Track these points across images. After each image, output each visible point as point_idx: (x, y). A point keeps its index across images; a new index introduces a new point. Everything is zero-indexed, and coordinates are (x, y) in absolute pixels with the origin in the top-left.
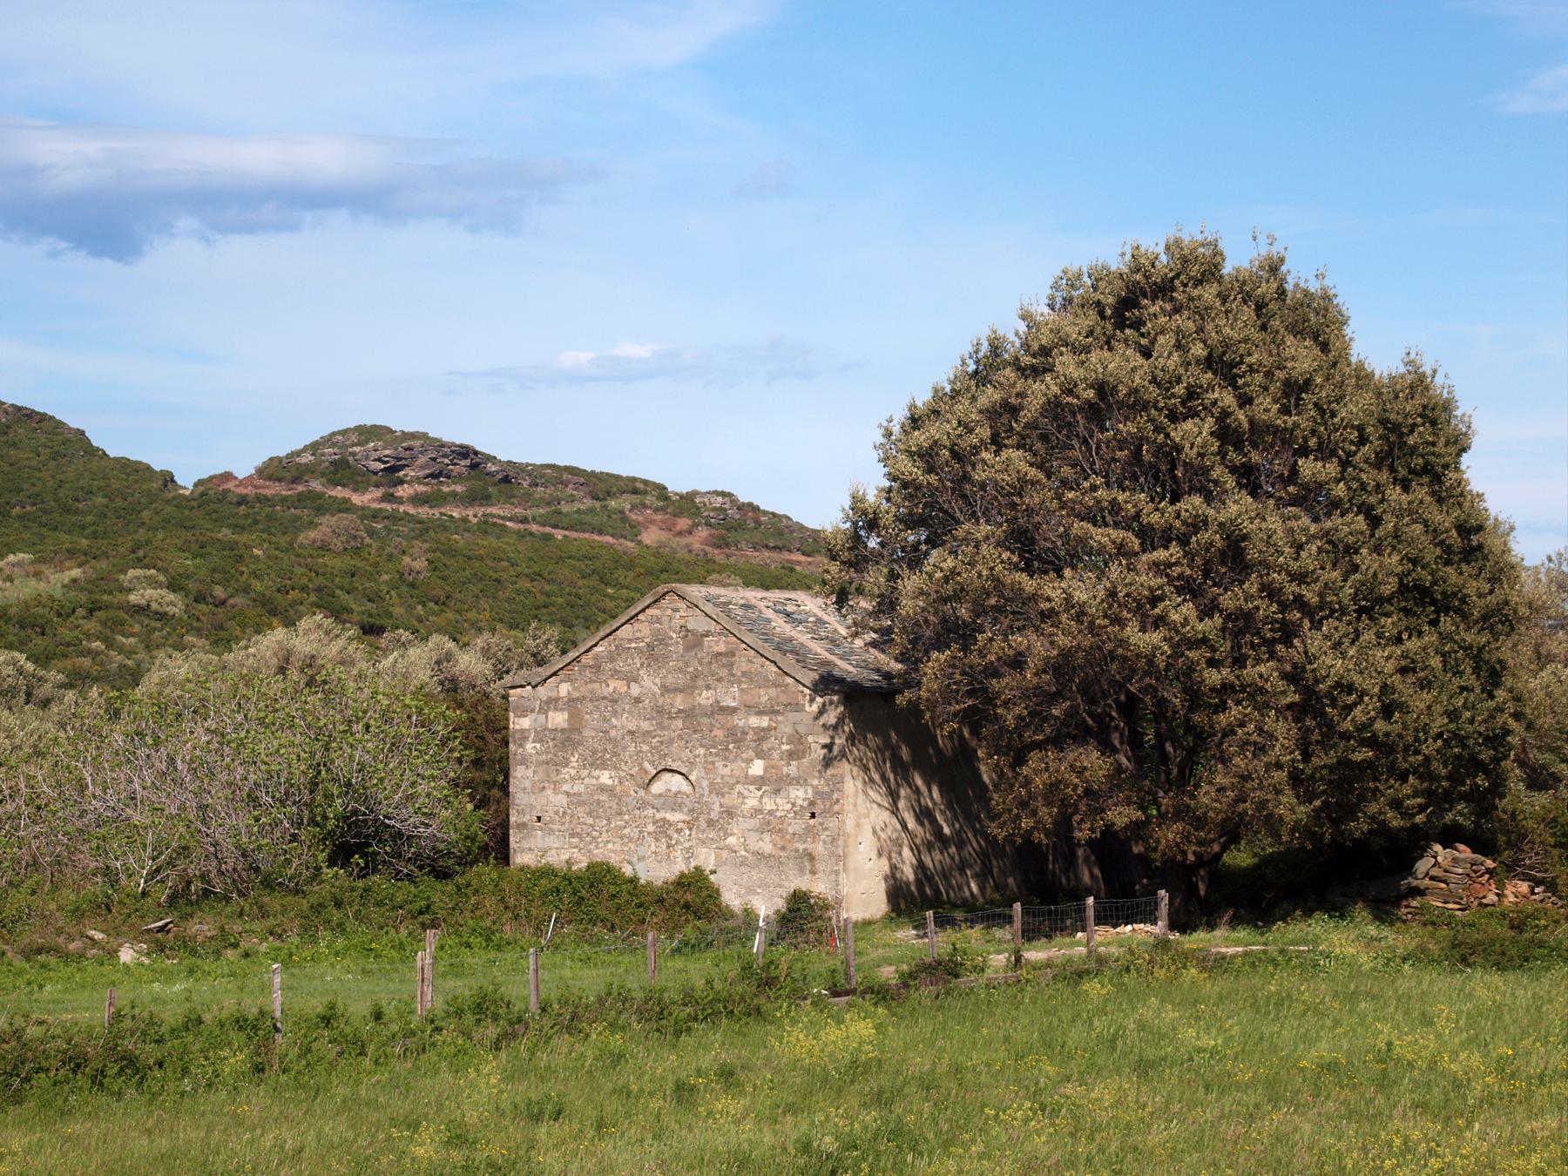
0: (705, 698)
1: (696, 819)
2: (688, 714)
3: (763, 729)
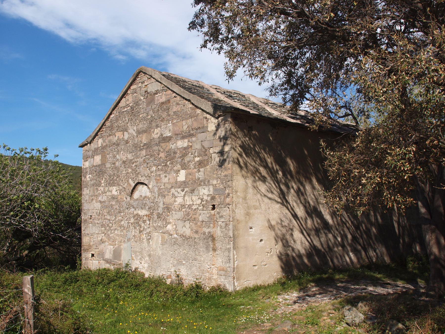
0: (156, 133)
1: (152, 214)
2: (148, 146)
3: (185, 149)
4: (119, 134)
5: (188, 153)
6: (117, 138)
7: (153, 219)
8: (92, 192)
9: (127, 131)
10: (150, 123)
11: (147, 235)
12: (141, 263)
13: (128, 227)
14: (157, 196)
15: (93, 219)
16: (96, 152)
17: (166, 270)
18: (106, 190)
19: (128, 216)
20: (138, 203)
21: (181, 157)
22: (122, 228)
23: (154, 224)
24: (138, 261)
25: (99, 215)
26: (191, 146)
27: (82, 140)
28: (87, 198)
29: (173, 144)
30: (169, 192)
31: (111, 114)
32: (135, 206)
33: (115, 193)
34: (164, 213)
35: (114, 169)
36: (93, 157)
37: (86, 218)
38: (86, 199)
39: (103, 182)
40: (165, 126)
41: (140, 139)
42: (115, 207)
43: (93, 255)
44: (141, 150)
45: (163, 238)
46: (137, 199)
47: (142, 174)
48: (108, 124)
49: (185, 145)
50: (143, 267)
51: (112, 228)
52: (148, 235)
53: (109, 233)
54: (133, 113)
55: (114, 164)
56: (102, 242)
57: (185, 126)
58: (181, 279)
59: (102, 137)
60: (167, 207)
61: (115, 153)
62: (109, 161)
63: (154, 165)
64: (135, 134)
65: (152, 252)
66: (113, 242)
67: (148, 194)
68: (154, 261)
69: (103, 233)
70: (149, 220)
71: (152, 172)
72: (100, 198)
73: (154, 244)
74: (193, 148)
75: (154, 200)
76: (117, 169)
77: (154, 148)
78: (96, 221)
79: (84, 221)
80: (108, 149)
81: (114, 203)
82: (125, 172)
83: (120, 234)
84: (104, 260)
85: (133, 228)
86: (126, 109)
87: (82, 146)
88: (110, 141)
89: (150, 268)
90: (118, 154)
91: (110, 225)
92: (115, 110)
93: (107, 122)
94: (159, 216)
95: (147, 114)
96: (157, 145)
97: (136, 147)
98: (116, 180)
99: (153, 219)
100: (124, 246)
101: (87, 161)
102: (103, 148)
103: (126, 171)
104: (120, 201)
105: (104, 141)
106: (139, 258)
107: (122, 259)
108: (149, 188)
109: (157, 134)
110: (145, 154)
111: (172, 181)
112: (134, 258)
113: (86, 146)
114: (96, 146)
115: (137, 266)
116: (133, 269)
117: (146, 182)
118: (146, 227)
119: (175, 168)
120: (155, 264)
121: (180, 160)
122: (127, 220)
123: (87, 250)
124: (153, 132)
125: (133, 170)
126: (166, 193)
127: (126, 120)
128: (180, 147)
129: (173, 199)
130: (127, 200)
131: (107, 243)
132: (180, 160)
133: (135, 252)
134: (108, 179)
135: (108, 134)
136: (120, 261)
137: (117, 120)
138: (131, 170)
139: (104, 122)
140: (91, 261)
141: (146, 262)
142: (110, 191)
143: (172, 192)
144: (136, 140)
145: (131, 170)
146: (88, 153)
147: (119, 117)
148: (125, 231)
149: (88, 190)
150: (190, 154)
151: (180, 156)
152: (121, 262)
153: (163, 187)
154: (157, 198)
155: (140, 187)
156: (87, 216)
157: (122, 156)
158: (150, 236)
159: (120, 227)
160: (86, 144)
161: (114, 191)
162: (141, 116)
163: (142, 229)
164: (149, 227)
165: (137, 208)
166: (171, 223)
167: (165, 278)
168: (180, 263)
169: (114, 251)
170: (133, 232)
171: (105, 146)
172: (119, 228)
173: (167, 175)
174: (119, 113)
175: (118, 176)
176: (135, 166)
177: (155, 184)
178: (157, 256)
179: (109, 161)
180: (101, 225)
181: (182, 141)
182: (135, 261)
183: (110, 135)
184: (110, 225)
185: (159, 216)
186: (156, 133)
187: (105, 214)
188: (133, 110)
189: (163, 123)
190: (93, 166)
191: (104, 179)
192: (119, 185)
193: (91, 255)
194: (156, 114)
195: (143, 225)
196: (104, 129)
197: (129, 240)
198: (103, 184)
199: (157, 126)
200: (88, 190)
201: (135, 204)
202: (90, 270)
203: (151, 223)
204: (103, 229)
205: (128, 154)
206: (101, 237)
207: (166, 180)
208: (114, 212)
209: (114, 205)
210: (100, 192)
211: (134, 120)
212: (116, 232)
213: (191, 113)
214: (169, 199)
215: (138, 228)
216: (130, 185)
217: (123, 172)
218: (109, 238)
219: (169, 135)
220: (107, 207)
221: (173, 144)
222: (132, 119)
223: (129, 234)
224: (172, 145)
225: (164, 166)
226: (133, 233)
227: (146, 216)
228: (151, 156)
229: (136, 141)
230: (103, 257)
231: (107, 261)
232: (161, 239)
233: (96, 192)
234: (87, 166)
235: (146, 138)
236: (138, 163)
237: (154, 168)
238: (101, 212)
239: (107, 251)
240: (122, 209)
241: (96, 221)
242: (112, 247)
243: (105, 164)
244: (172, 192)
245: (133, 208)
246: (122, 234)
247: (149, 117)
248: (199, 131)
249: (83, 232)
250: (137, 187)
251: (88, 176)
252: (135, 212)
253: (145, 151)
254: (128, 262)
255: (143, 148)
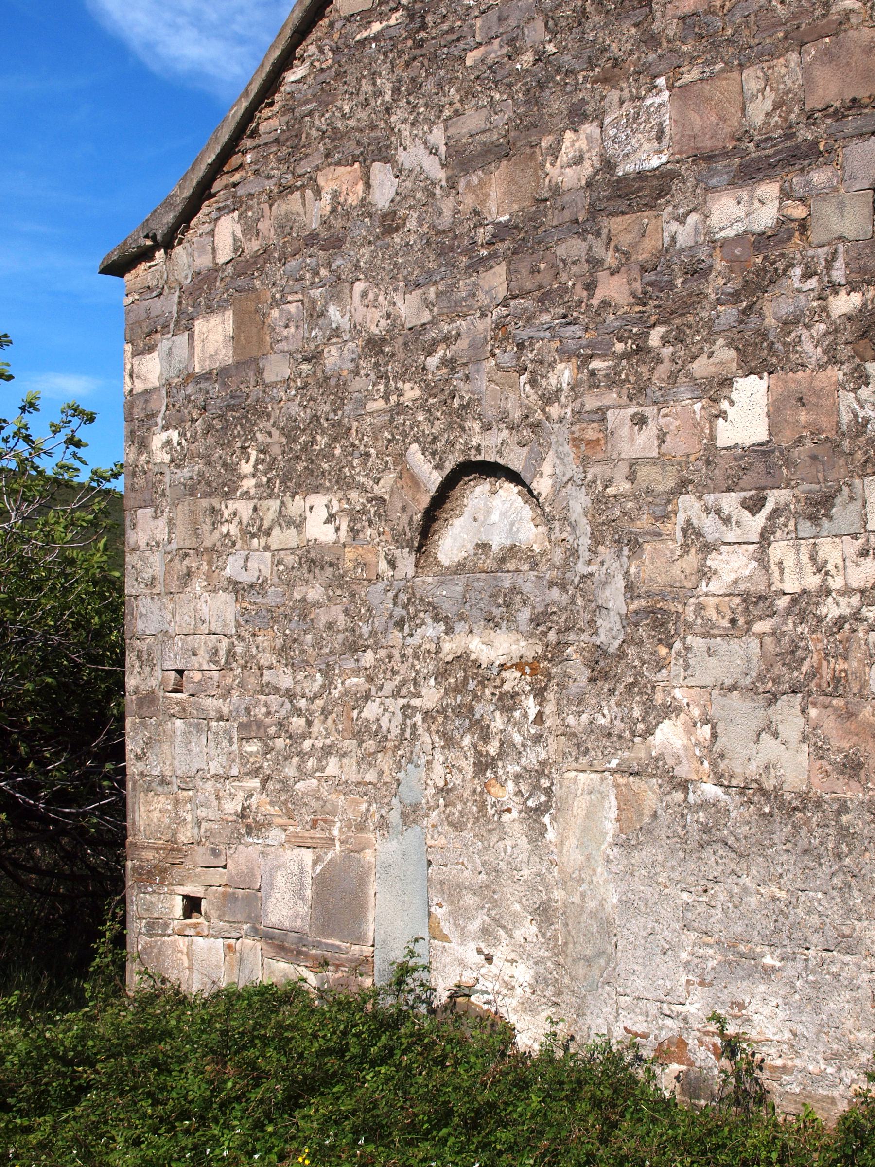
0: (571, 159)
1: (555, 653)
2: (521, 238)
3: (762, 241)
4: (339, 181)
5: (780, 265)
6: (325, 204)
7: (562, 686)
8: (181, 530)
9: (386, 160)
10: (533, 99)
11: (524, 788)
12: (489, 959)
13: (408, 736)
14: (585, 542)
15: (188, 687)
16: (202, 294)
17: (653, 1008)
18: (269, 517)
19: (403, 669)
20: (467, 588)
21: (735, 297)
22: (370, 744)
23: (571, 720)
24: (473, 945)
25: (227, 667)
26: (803, 225)
27: (128, 233)
28: (156, 565)
29: (681, 220)
30: (665, 517)
31: (285, 62)
32: (448, 608)
33: (319, 531)
34: (631, 651)
35: (313, 391)
36: (185, 323)
37: (153, 682)
38: (147, 575)
39: (246, 468)
40: (629, 108)
41: (469, 201)
42: (322, 617)
43: (192, 905)
44: (478, 265)
45: (627, 803)
46: (459, 568)
47: (491, 414)
48: (270, 123)
49: (766, 217)
50: (504, 985)
51: (307, 744)
52: (536, 788)
53: (290, 771)
54: (420, 44)
55: (315, 357)
56: (248, 824)
57: (757, 99)
58: (754, 1066)
59: (237, 205)
60: (650, 611)
61: (316, 293)
62: (283, 346)
63: (565, 354)
64: (441, 175)
65: (558, 894)
66: (314, 824)
67: (530, 534)
68: (575, 950)
69: (255, 772)
70: (540, 694)
71: (549, 398)
72: (232, 567)
73: (572, 842)
74: (815, 236)
75: (566, 566)
76: (334, 387)
77: (561, 251)
78: (212, 704)
79: (141, 703)
80: (277, 272)
81: (315, 593)
82: (381, 404)
83: (354, 777)
84: (256, 932)
85: (439, 742)
86: (376, 27)
87: (117, 268)
88: (284, 226)
89: (548, 987)
90: (335, 296)
91: (298, 723)
92: (313, 36)
93: (267, 113)
94: (602, 666)
95: (511, 42)
96: (579, 228)
97: (443, 251)
98: (327, 454)
99: (562, 686)
100: (381, 850)
101: (151, 349)
102: (247, 266)
103: (386, 397)
104: (357, 580)
105: (250, 229)
106: (474, 926)
107: (370, 928)
108: (531, 495)
109: (578, 161)
110: (502, 292)
111: (680, 445)
112: (446, 928)
113: (143, 266)
114: (204, 262)
115: (467, 978)
116: (442, 997)
117: (515, 460)
118: (517, 738)
119: (701, 367)
120: (581, 970)
121: (729, 314)
122: (396, 694)
123: (157, 875)
124: (555, 151)
125: (429, 389)
126: (644, 522)
127: (379, 93)
128: (730, 233)
129: (692, 560)
130: (399, 574)
131: (276, 835)
132: (729, 314)
133: (453, 891)
134: (276, 450)
135: (270, 185)
136: (359, 940)
137: (325, 96)
138: (417, 393)
139: (249, 116)
140: (182, 942)
141: (522, 951)
142: (291, 523)
143: (681, 519)
144: (447, 206)
145: (417, 393)
146: (157, 306)
147: (339, 75)
148: (385, 762)
149: (162, 522)
150: (798, 271)
151: (730, 288)
152: (367, 950)
153: (625, 486)
154: (585, 554)
155: (477, 494)
156: (158, 673)
157: (361, 310)
158: (548, 792)
159: (359, 736)
160: (146, 255)
161: (318, 520)
162: (471, 59)
163: (493, 749)
164: (538, 739)
165: (462, 618)
166: (678, 710)
167: (647, 1053)
168: (740, 961)
169: (322, 883)
170: (437, 767)
171: (256, 256)
172: (349, 744)
173: (650, 411)
174: (336, 50)
175: (340, 432)
176: (444, 362)
177: (573, 469)
178: (594, 915)
179: (283, 346)
180: (242, 727)
181: (744, 194)
182: (455, 947)
183: (285, 190)
184: (298, 723)
185: (602, 666)
186: (571, 159)
187: (266, 659)
188: (423, 27)
189: (614, 95)
190: (190, 377)
191: (253, 454)
192: (344, 483)
193: (178, 905)
194: (569, 40)
195: (498, 722)
196: (249, 158)
197: (411, 815)
198: (248, 484)
199: (577, 116)
200: (162, 522)
201: (447, 595)
202: (180, 1000)
203: (550, 708)
204: (253, 747)
205: (398, 298)
206: (241, 796)
207: (642, 443)
208: (318, 644)
209: (317, 604)
210: (234, 529)
211: (429, 86)
212: (332, 766)
213: (795, 16)
214: (661, 563)
215: (466, 741)
216: (416, 483)
217: (371, 406)
218: (290, 804)
219: (655, 162)
220: (272, 616)
221: (681, 220)
222: (416, 86)
223: (411, 776)
224: (674, 226)
225: (626, 355)
226: (439, 770)
227: (519, 666)
228: (545, 298)
229: (447, 213)
230: (254, 919)
231: (280, 943)
232: (613, 814)
233: (207, 527)
234: (154, 381)
235: (509, 193)
236: (463, 344)
237: (564, 374)
238: (239, 649)
239: (280, 881)
240: (365, 630)
241: (212, 704)
242: (308, 856)
243: (256, 360)
244: (681, 519)
245: (436, 619)
246: (371, 776)
247: (528, 58)
248: (851, 124)
249: (133, 767)
250: (456, 492)
251: (157, 440)
252: (447, 647)
253: (500, 270)
254: (411, 954)
255: (492, 256)
